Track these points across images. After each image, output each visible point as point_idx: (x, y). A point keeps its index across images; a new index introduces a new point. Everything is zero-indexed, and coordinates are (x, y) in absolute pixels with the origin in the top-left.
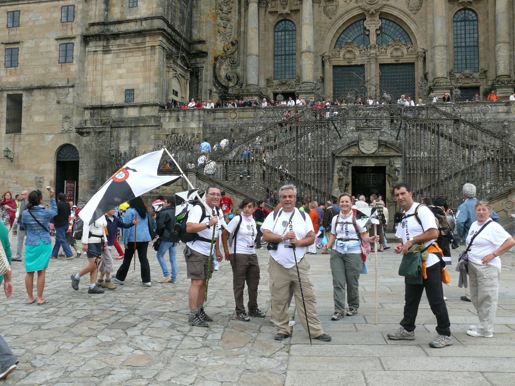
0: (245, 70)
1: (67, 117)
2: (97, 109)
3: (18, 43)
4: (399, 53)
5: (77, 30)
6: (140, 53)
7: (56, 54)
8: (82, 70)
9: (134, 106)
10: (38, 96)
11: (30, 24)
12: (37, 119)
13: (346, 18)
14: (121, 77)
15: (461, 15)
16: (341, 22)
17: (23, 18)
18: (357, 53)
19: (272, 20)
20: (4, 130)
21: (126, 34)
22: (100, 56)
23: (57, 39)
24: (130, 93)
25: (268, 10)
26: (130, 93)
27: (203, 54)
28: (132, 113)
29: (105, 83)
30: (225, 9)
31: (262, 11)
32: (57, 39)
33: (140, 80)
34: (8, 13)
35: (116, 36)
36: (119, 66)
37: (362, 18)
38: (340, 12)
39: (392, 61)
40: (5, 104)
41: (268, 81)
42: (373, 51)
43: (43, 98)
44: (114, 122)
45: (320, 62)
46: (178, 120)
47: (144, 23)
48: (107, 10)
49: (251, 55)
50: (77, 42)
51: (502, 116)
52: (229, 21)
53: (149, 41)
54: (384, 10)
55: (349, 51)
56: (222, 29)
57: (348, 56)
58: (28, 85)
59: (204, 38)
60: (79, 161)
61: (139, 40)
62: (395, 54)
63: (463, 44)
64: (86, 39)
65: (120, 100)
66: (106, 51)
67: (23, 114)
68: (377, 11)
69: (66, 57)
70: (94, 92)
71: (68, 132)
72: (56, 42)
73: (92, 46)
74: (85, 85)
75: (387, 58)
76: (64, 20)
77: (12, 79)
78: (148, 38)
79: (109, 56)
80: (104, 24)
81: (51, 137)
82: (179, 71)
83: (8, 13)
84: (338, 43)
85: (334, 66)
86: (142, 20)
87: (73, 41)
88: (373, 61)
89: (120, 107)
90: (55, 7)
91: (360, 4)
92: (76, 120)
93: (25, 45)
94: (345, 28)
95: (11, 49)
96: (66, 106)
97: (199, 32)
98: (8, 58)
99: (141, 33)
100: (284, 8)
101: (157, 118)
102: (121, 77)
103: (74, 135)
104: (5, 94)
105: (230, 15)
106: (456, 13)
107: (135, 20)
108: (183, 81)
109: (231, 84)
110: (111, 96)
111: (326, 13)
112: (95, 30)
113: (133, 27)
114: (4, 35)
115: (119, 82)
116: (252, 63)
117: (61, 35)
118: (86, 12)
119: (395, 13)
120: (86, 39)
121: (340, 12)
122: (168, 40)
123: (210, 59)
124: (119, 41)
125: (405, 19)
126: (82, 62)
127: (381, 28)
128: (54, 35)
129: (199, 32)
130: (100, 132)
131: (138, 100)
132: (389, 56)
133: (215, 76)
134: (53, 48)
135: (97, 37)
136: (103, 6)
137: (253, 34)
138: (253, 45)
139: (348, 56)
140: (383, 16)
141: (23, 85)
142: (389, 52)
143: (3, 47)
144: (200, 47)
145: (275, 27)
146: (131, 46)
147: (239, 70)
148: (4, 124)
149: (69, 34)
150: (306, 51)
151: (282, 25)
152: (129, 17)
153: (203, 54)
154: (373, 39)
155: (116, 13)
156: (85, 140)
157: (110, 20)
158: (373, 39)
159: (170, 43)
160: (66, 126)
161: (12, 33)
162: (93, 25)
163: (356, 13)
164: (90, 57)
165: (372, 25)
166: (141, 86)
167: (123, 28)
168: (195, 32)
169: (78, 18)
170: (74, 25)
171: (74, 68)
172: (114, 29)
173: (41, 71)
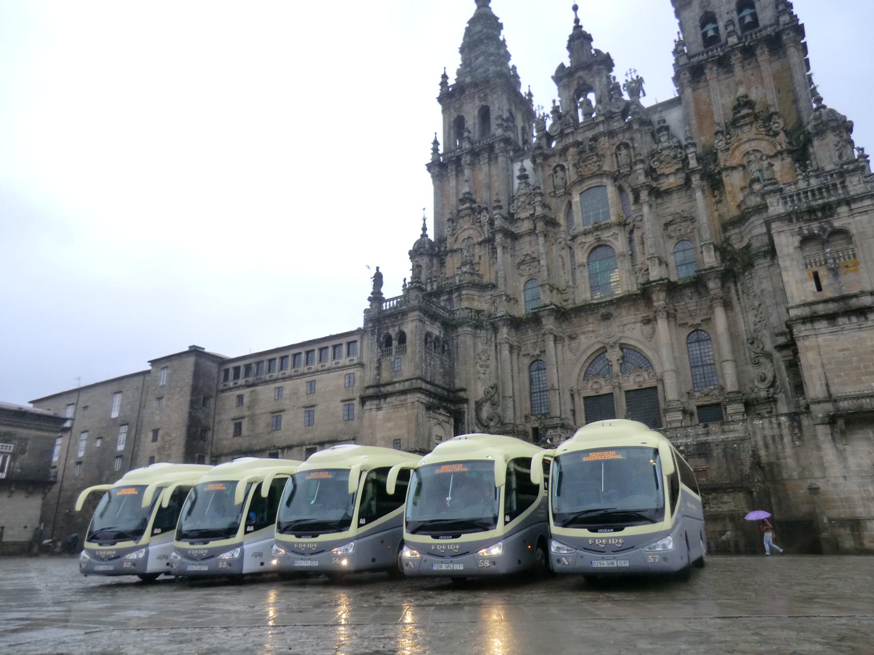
0: (504, 410)
3: (313, 406)
4: (641, 379)
5: (357, 395)
6: (404, 409)
7: (341, 413)
13: (589, 353)
15: (694, 337)
16: (585, 358)
17: (318, 386)
19: (527, 361)
21: (392, 394)
22: (374, 412)
23: (342, 401)
25: (522, 353)
30: (484, 358)
31: (515, 356)
32: (342, 401)
35: (385, 396)
37: (603, 350)
38: (583, 347)
39: (636, 387)
41: (526, 417)
47: (406, 383)
48: (379, 374)
50: (356, 403)
51: (703, 438)
52: (487, 367)
53: (410, 398)
54: (622, 341)
55: (596, 382)
56: (482, 376)
58: (321, 440)
59: (464, 386)
61: (403, 398)
63: (700, 364)
64: (363, 400)
66: (379, 409)
68: (615, 343)
69: (349, 416)
72: (342, 404)
73: (368, 405)
75: (631, 383)
76: (347, 385)
77: (309, 436)
78: (409, 396)
79: (380, 413)
80: (378, 386)
84: (586, 376)
86: (404, 381)
87: (353, 402)
88: (617, 389)
91: (599, 339)
94: (590, 361)
98: (307, 419)
99: (404, 392)
100: (535, 350)
104: (304, 448)
105: (488, 362)
106: (689, 335)
111: (571, 350)
112: (370, 392)
113: (398, 387)
114: (305, 401)
117: (345, 398)
118: (362, 379)
119: (632, 342)
120: (363, 400)
121: (583, 347)
122: (427, 395)
124: (388, 400)
125: (641, 347)
126: (361, 418)
127: (623, 358)
128: (341, 398)
132: (632, 382)
136: (375, 372)
139: (595, 386)
140: (622, 347)
141: (317, 440)
143: (303, 410)
144: (462, 394)
145: (530, 367)
146: (396, 403)
147: (499, 410)
149: (350, 396)
151: (535, 366)
152: (395, 380)
153: (466, 401)
154: (616, 368)
155: (386, 376)
157: (383, 381)
158: (616, 368)
159: (430, 397)
161: (310, 398)
162: (368, 387)
163: (597, 347)
164: (367, 414)
165: (614, 355)
167: (389, 389)
168: (456, 381)
169: (357, 384)
171: (355, 423)
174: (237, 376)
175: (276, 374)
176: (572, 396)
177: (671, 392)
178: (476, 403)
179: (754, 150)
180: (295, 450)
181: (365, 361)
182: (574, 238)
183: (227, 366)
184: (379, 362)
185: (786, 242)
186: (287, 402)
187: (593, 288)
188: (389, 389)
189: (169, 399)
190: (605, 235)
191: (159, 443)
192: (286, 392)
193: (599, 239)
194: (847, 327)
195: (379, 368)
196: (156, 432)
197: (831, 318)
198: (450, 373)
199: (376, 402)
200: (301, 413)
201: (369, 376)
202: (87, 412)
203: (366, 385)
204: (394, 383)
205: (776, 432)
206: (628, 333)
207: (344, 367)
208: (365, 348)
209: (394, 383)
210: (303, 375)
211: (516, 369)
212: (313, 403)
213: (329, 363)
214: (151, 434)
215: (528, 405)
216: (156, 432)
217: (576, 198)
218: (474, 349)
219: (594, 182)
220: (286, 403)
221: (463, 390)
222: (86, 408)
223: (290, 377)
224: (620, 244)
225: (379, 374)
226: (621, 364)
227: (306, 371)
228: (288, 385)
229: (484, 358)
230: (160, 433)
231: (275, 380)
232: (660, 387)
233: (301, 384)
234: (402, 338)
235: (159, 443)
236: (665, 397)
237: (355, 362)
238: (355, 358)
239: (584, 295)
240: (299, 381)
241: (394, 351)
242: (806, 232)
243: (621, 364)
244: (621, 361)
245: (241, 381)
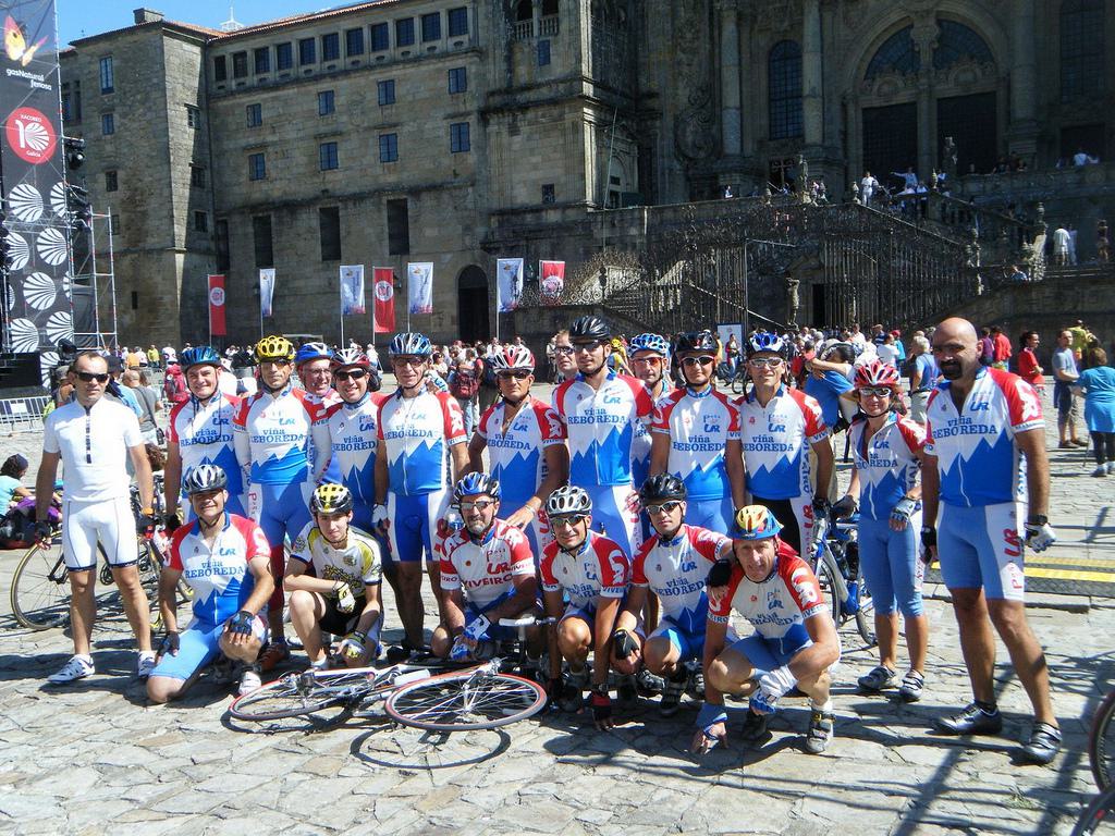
1: (467, 229)
2: (508, 214)
3: (395, 125)
4: (969, 76)
5: (473, 105)
7: (446, 140)
8: (484, 160)
9: (556, 208)
10: (428, 200)
11: (410, 98)
12: (429, 232)
14: (535, 167)
17: (399, 91)
18: (900, 84)
20: (387, 251)
21: (537, 104)
24: (548, 189)
25: (756, 27)
26: (548, 189)
27: (656, 114)
28: (553, 217)
29: (516, 177)
33: (559, 171)
34: (379, 83)
35: (524, 108)
36: (532, 152)
40: (385, 214)
41: (761, 142)
42: (923, 80)
43: (434, 203)
44: (530, 232)
45: (836, 108)
46: (613, 225)
48: (511, 70)
49: (727, 108)
50: (473, 120)
56: (685, 70)
57: (886, 88)
60: (487, 288)
61: (555, 112)
62: (962, 78)
64: (484, 115)
65: (537, 199)
66: (514, 131)
67: (410, 226)
69: (460, 141)
70: (501, 192)
72: (445, 123)
74: (488, 182)
75: (948, 88)
77: (392, 178)
79: (517, 139)
80: (509, 90)
81: (449, 256)
82: (621, 146)
83: (379, 83)
85: (865, 110)
89: (536, 210)
90: (439, 70)
92: (481, 230)
93: (406, 129)
95: (388, 135)
96: (466, 213)
97: (648, 80)
99: (553, 102)
100: (782, 21)
102: (535, 167)
103: (478, 252)
104: (384, 200)
107: (548, 83)
108: (627, 160)
109: (702, 154)
110: (524, 195)
112: (496, 101)
113: (545, 93)
114: (377, 116)
115: (535, 175)
116: (731, 119)
117: (450, 110)
118: (481, 76)
120: (484, 115)
123: (669, 121)
124: (530, 115)
126: (482, 148)
128: (441, 114)
129: (648, 80)
130: (513, 247)
131: (560, 199)
133: (677, 146)
134: (439, 128)
135: (498, 110)
136: (504, 66)
137: (730, 75)
138: (731, 97)
142: (952, 77)
144: (653, 103)
145: (770, 53)
148: (386, 242)
150: (808, 96)
152: (539, 80)
153: (656, 114)
155: (523, 73)
158: (926, 58)
160: (468, 241)
161: (386, 112)
162: (492, 93)
166: (563, 179)
167: (532, 95)
168: (643, 80)
169: (472, 86)
170: (468, 96)
171: (472, 158)
172: (521, 98)
173: (428, 165)
174: (240, 71)
175: (316, 67)
176: (844, 106)
177: (1023, 101)
178: (676, 118)
180: (368, 205)
181: (482, 43)
186: (345, 118)
188: (532, 95)
189: (124, 115)
191: (122, 192)
192: (340, 101)
195: (509, 59)
199: (508, 119)
200: (373, 140)
201: (495, 73)
203: (493, 87)
204: (539, 86)
207: (445, 55)
208: (482, 22)
209: (539, 86)
210: (370, 68)
211: (746, 56)
212: (394, 120)
213: (418, 47)
214: (102, 179)
215: (765, 122)
218: (673, 20)
220: (342, 120)
221: (652, 95)
223: (346, 73)
225: (511, 70)
226: (935, 51)
227: (373, 62)
228: (343, 88)
229: (689, 36)
230: (121, 175)
231: (318, 78)
232: (1001, 94)
233: (365, 85)
235: (122, 192)
236: (1009, 113)
237: (466, 45)
238: (464, 38)
240: (362, 81)
243: (935, 51)
244: (936, 46)
245: (252, 79)
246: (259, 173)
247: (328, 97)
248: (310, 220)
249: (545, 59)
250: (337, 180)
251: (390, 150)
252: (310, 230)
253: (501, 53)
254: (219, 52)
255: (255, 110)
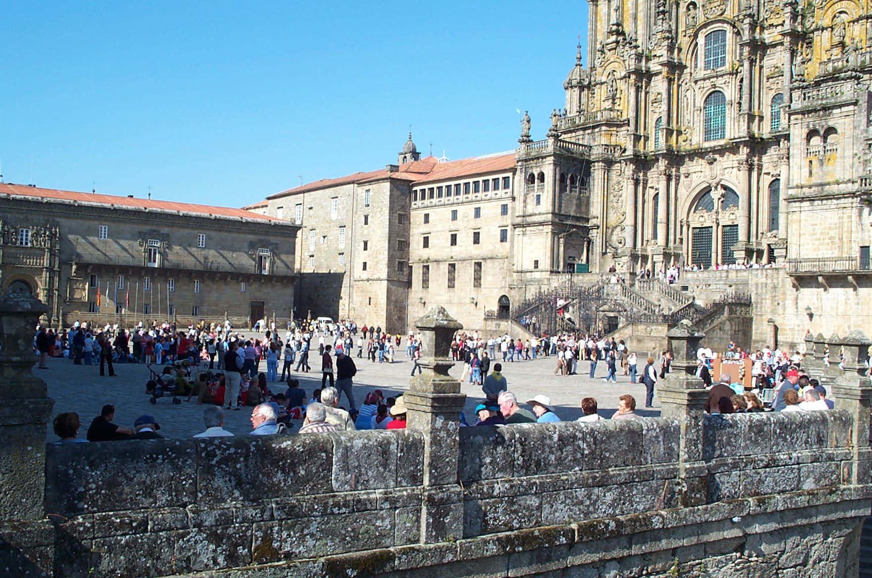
5: (509, 222)
26: (536, 262)
35: (529, 225)
48: (525, 207)
50: (509, 228)
61: (541, 227)
71: (505, 287)
101: (549, 280)
103: (507, 289)
139: (702, 219)
140: (725, 187)
149: (505, 224)
155: (530, 210)
156: (513, 292)
157: (528, 214)
165: (716, 194)
172: (529, 219)
179: (841, 13)
182: (696, 82)
183: (414, 189)
184: (526, 196)
185: (798, 133)
187: (708, 134)
190: (720, 82)
193: (714, 86)
194: (819, 207)
196: (366, 243)
197: (811, 200)
198: (584, 203)
201: (518, 207)
202: (311, 212)
204: (536, 215)
205: (764, 280)
206: (726, 176)
214: (362, 244)
216: (366, 243)
217: (701, 40)
219: (717, 26)
222: (311, 208)
224: (730, 92)
225: (525, 207)
234: (542, 177)
239: (696, 138)
241: (536, 188)
242: (811, 126)
246: (426, 243)
247: (455, 213)
248: (445, 267)
249: (538, 202)
250: (456, 252)
251: (476, 240)
252: (444, 273)
253: (522, 198)
254: (414, 189)
255: (427, 216)
